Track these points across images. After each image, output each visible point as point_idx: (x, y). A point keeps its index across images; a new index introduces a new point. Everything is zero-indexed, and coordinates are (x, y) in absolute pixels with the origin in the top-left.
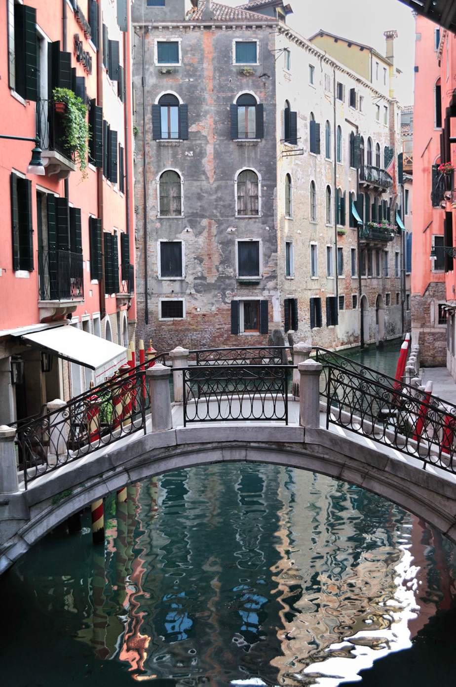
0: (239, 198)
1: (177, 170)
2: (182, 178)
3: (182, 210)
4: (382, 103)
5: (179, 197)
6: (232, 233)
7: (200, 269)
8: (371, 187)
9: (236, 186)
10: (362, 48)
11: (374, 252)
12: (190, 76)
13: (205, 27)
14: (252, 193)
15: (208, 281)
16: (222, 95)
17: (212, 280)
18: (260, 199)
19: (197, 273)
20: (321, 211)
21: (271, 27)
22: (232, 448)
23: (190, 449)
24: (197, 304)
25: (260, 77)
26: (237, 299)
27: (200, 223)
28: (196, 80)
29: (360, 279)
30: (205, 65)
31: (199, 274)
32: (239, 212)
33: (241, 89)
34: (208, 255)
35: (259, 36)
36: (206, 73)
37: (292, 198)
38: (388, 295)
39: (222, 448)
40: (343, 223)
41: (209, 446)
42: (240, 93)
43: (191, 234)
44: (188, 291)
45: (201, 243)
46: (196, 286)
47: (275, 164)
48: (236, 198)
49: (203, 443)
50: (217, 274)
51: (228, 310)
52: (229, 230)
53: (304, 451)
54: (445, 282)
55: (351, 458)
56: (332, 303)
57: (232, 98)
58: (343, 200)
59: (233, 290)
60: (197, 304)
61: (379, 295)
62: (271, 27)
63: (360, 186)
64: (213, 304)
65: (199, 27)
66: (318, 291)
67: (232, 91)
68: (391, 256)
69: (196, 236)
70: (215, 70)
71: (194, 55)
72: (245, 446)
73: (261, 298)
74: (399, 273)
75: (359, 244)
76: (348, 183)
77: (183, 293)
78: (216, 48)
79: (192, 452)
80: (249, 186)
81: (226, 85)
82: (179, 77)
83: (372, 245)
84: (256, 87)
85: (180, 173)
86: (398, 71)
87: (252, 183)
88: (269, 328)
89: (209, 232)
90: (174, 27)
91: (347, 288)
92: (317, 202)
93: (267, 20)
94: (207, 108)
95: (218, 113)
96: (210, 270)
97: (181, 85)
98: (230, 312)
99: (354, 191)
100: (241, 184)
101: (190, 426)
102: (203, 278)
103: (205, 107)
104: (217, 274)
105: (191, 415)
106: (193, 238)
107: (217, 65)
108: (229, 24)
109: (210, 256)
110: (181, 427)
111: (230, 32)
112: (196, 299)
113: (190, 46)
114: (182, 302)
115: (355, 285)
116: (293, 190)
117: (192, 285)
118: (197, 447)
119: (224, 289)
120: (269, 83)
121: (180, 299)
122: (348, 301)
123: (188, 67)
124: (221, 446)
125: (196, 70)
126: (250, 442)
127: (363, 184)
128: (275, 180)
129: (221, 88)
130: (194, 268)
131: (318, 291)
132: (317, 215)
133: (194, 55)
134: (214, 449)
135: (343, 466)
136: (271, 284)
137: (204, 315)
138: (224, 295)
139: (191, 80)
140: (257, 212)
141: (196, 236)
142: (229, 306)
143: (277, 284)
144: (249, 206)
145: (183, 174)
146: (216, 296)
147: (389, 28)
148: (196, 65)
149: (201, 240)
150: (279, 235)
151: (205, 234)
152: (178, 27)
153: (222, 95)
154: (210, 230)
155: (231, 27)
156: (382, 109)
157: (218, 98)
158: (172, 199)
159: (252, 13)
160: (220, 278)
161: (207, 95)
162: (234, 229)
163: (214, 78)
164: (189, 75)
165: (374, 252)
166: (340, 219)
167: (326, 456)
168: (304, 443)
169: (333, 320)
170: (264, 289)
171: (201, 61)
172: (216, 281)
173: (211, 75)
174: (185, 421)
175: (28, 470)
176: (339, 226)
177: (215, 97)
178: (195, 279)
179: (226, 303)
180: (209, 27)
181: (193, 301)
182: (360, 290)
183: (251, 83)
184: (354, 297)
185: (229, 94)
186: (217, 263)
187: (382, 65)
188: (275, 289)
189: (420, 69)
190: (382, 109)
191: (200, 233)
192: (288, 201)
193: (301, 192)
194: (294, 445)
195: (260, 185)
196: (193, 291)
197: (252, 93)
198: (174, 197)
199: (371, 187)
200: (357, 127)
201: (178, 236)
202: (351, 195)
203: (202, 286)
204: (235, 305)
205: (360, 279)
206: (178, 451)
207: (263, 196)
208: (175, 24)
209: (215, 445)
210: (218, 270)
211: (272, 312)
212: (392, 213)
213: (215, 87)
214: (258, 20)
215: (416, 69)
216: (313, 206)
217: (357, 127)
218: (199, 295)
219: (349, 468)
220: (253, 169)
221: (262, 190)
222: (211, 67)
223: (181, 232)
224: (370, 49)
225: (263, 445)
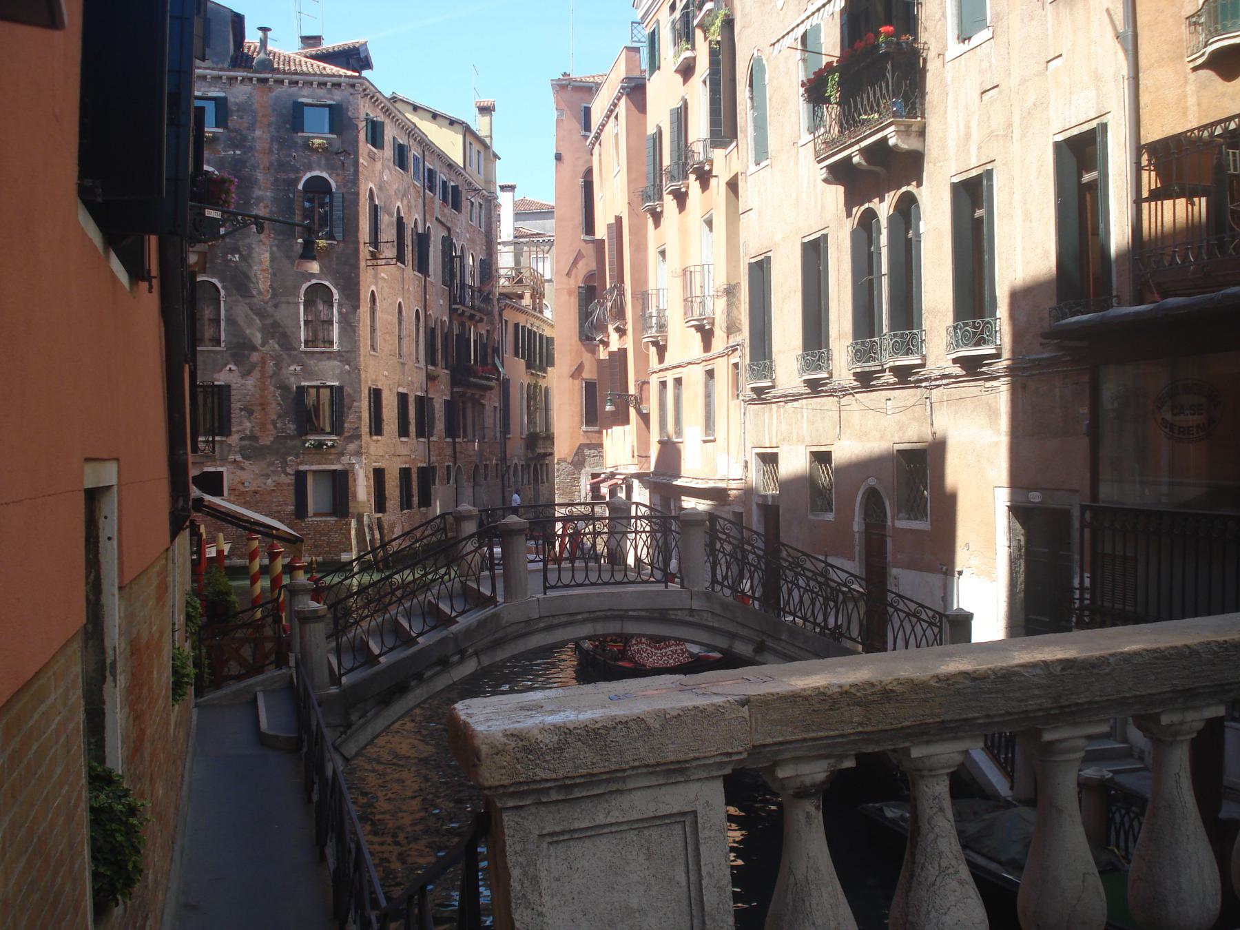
0: (306, 322)
1: (215, 281)
2: (222, 292)
3: (223, 338)
4: (477, 200)
5: (218, 321)
6: (295, 373)
7: (248, 425)
8: (467, 314)
9: (302, 307)
10: (452, 122)
11: (469, 405)
12: (235, 147)
13: (259, 80)
14: (323, 317)
15: (261, 442)
16: (281, 176)
17: (266, 441)
18: (336, 326)
19: (244, 430)
20: (409, 346)
21: (353, 86)
22: (606, 618)
23: (556, 622)
24: (244, 475)
25: (337, 154)
26: (302, 468)
27: (248, 358)
28: (244, 153)
29: (454, 443)
30: (258, 133)
31: (248, 432)
32: (306, 343)
33: (310, 170)
34: (261, 404)
35: (336, 98)
36: (258, 145)
37: (378, 325)
38: (486, 466)
39: (594, 620)
40: (434, 363)
41: (580, 617)
42: (308, 175)
43: (237, 373)
44: (231, 458)
45: (250, 387)
46: (243, 451)
47: (358, 276)
48: (302, 323)
49: (571, 614)
50: (274, 432)
51: (289, 485)
52: (292, 368)
53: (691, 619)
54: (601, 445)
55: (743, 626)
56: (426, 475)
57: (297, 180)
58: (433, 331)
59: (297, 456)
60: (244, 475)
61: (476, 466)
62: (353, 86)
63: (452, 312)
64: (268, 476)
65: (251, 79)
66: (407, 459)
67: (297, 171)
68: (488, 411)
69: (243, 376)
70: (272, 140)
71: (242, 118)
72: (623, 616)
73: (338, 467)
74: (498, 435)
75: (452, 393)
76: (439, 310)
77: (224, 461)
78: (274, 110)
79: (559, 626)
80: (321, 306)
81: (288, 162)
82: (220, 148)
83: (469, 394)
84: (331, 168)
85: (219, 285)
86: (496, 157)
87: (324, 302)
88: (351, 510)
89: (263, 371)
90: (213, 78)
91: (439, 455)
92: (404, 333)
93: (346, 77)
94: (261, 193)
95: (275, 200)
96: (263, 426)
97: (222, 159)
98: (292, 488)
99: (445, 318)
100: (309, 304)
101: (551, 594)
102: (253, 437)
103: (258, 193)
104: (274, 432)
105: (552, 578)
106: (239, 379)
107: (275, 133)
108: (295, 77)
109: (263, 406)
110: (541, 596)
111: (294, 89)
112: (243, 469)
113: (237, 104)
114: (221, 473)
115: (449, 451)
116: (378, 314)
117: (237, 449)
118: (563, 619)
119: (288, 454)
120: (348, 163)
121: (220, 469)
122: (440, 474)
123: (233, 135)
124: (594, 617)
125: (244, 139)
126: (627, 611)
127: (457, 310)
128: (358, 300)
129: (281, 166)
130: (241, 424)
131: (407, 459)
132: (405, 350)
133: (242, 118)
134: (585, 621)
135: (733, 636)
136: (352, 447)
137: (256, 492)
138: (284, 464)
139: (238, 152)
140: (332, 343)
141: (243, 376)
142: (289, 480)
143: (361, 447)
144: (321, 336)
145: (224, 287)
146: (272, 464)
147: (486, 100)
148: (244, 132)
149: (251, 382)
150: (363, 376)
151: (256, 374)
152: (220, 77)
153: (281, 176)
154: (263, 368)
155: (297, 83)
156: (476, 210)
157: (276, 179)
158: (207, 323)
159: (322, 64)
160: (277, 438)
161: (260, 176)
162: (298, 368)
163: (271, 152)
164: (235, 146)
165: (469, 405)
166: (431, 358)
167: (716, 625)
168: (692, 611)
169: (426, 501)
170: (343, 454)
171: (252, 128)
172: (273, 442)
173: (267, 146)
174: (545, 588)
175: (376, 651)
176: (430, 367)
177: (272, 179)
178: (242, 439)
179: (287, 474)
180: (266, 80)
181: (239, 472)
182: (455, 457)
183: (323, 162)
184: (448, 467)
185: (293, 176)
186: (274, 417)
187: (476, 147)
188: (358, 453)
189: (565, 156)
190: (476, 210)
191: (249, 373)
192: (373, 330)
193: (385, 316)
194: (679, 613)
195: (335, 306)
196: (239, 458)
197: (325, 175)
198: (210, 320)
199: (467, 314)
200: (449, 230)
201: (216, 376)
202: (443, 322)
203: (253, 451)
204: (301, 477)
205: (454, 443)
206: (542, 625)
207: (340, 323)
208: (215, 73)
209: (586, 615)
210: (275, 427)
211: (355, 486)
212: (489, 350)
213: (271, 164)
214: (334, 76)
215: (558, 157)
216: (400, 338)
217: (449, 230)
218: (247, 462)
219: (741, 638)
220: (327, 283)
221: (340, 313)
222: (267, 136)
223: (220, 371)
224: (462, 123)
225: (643, 613)
